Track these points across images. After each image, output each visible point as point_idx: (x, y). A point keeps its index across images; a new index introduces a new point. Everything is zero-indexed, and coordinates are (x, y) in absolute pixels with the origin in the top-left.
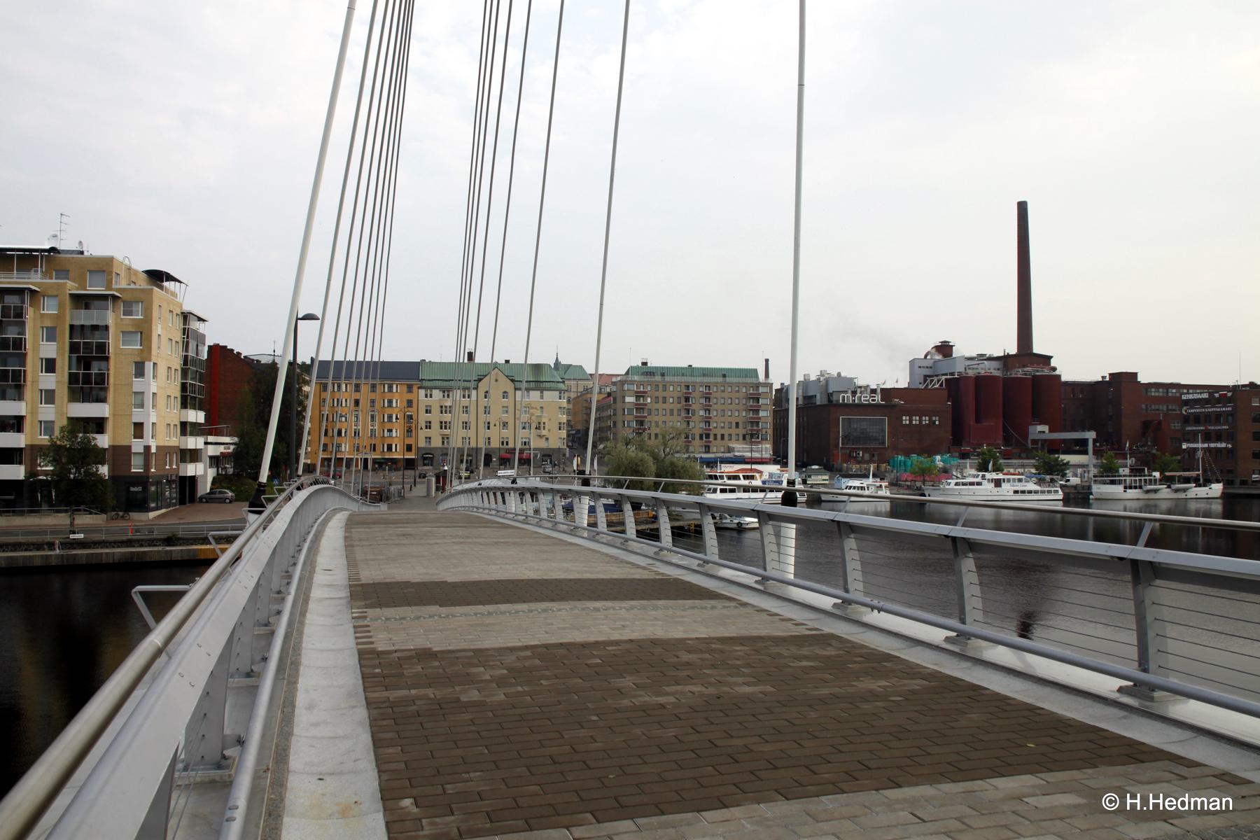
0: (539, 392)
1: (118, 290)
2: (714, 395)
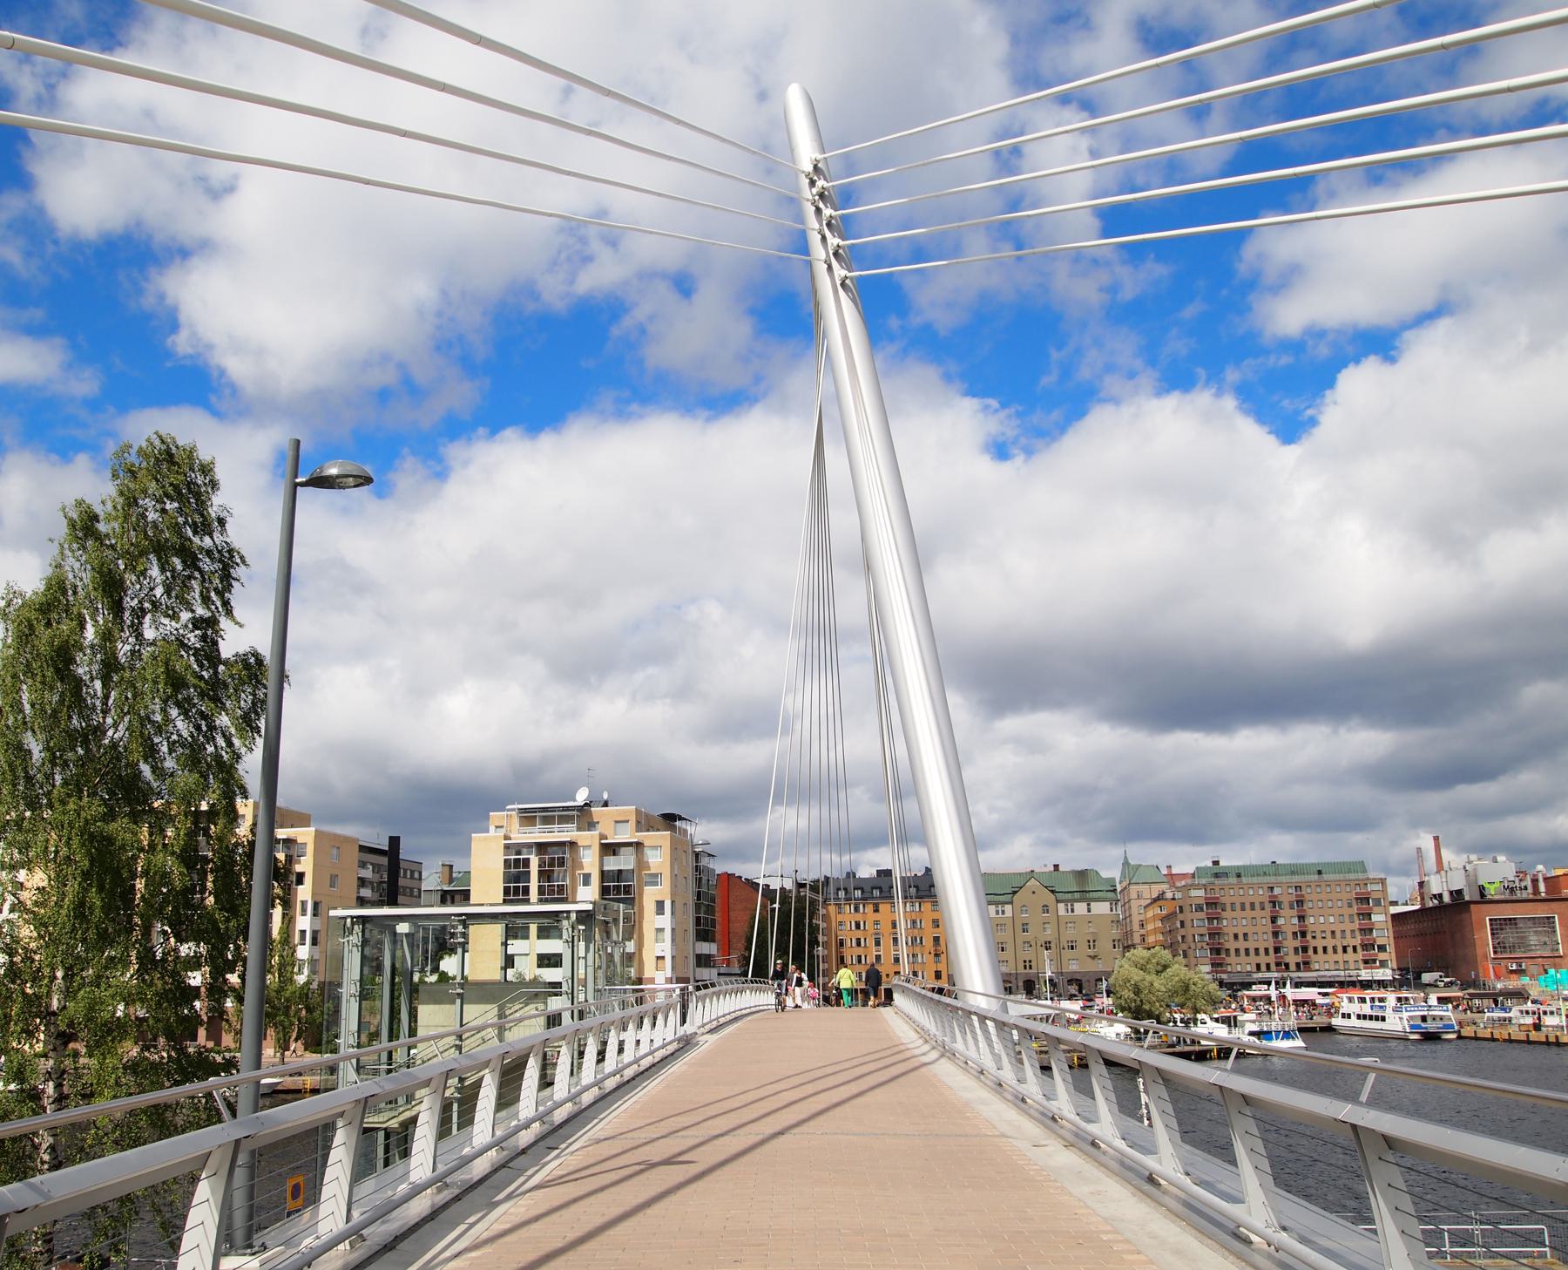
0: (1085, 904)
2: (1308, 897)
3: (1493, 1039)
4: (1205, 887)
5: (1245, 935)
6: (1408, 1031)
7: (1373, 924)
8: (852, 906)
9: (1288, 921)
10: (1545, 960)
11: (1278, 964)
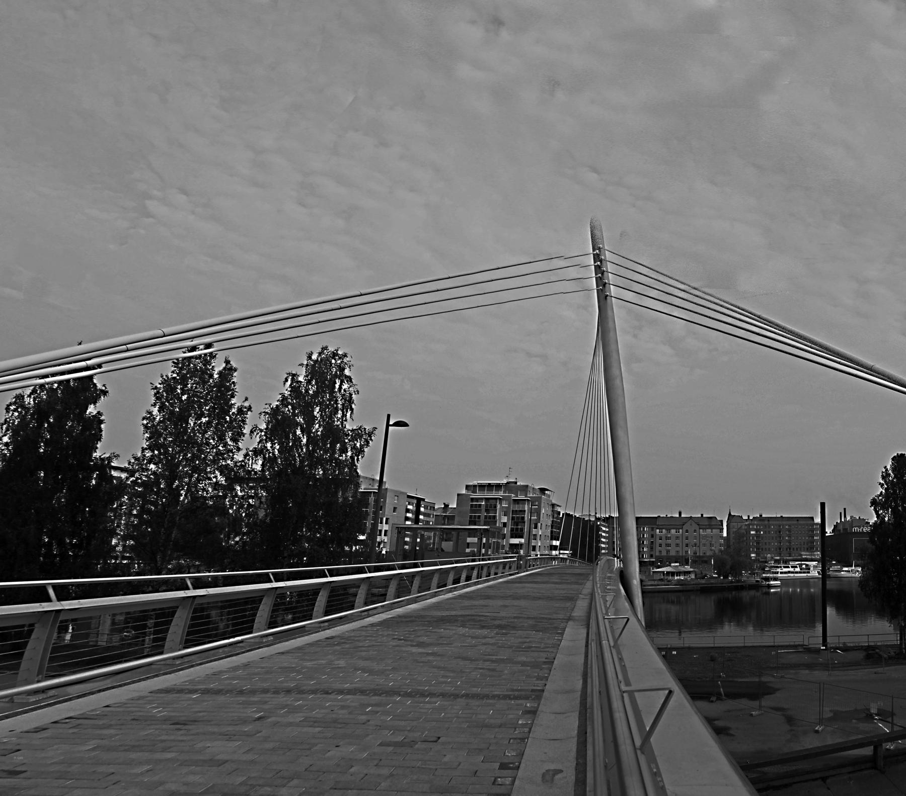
1: (529, 497)
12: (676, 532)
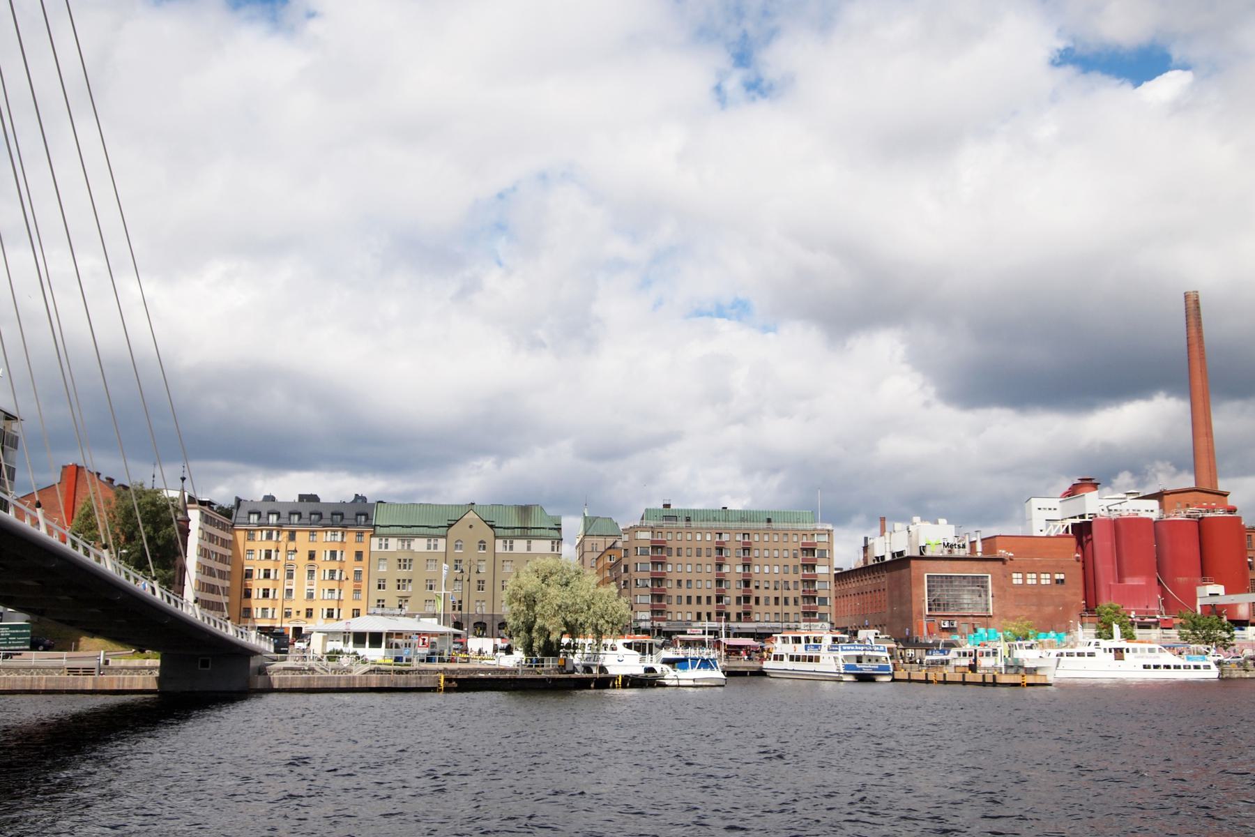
0: (525, 542)
2: (754, 546)
3: (927, 681)
4: (652, 529)
5: (689, 581)
6: (842, 671)
7: (816, 576)
8: (264, 532)
9: (733, 569)
10: (976, 619)
11: (719, 614)
12: (429, 548)
